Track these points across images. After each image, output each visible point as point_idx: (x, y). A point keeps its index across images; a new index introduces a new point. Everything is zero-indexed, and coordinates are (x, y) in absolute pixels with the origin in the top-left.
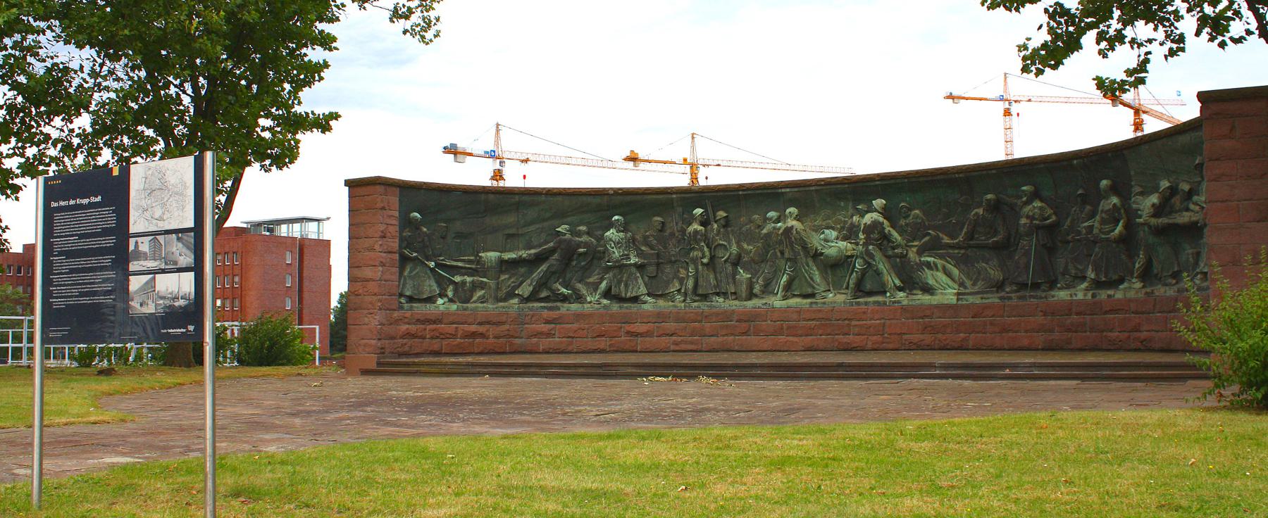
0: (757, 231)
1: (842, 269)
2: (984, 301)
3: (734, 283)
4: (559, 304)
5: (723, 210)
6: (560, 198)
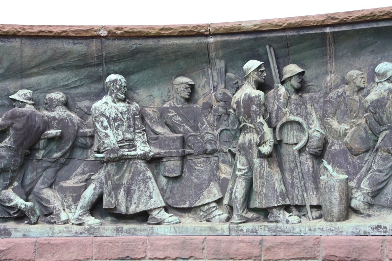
0: (356, 97)
3: (317, 188)
4: (10, 225)
5: (294, 62)
6: (16, 43)
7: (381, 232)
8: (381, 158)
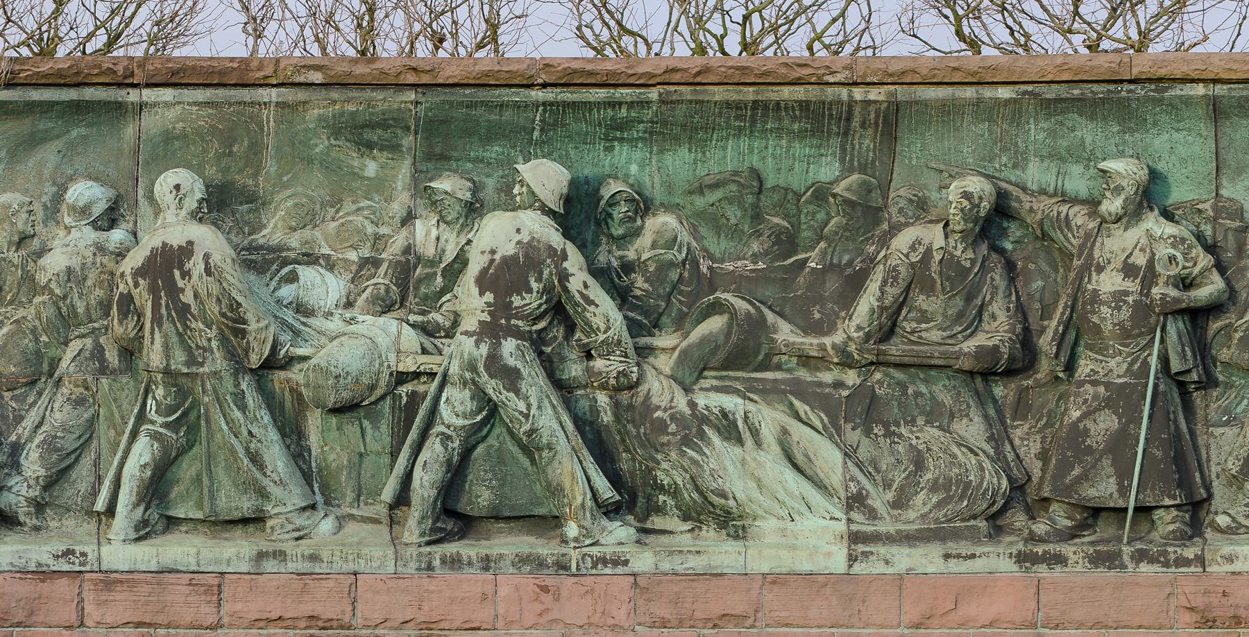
0: (14, 257)
1: (366, 423)
2: (954, 566)
7: (73, 563)
8: (68, 399)
